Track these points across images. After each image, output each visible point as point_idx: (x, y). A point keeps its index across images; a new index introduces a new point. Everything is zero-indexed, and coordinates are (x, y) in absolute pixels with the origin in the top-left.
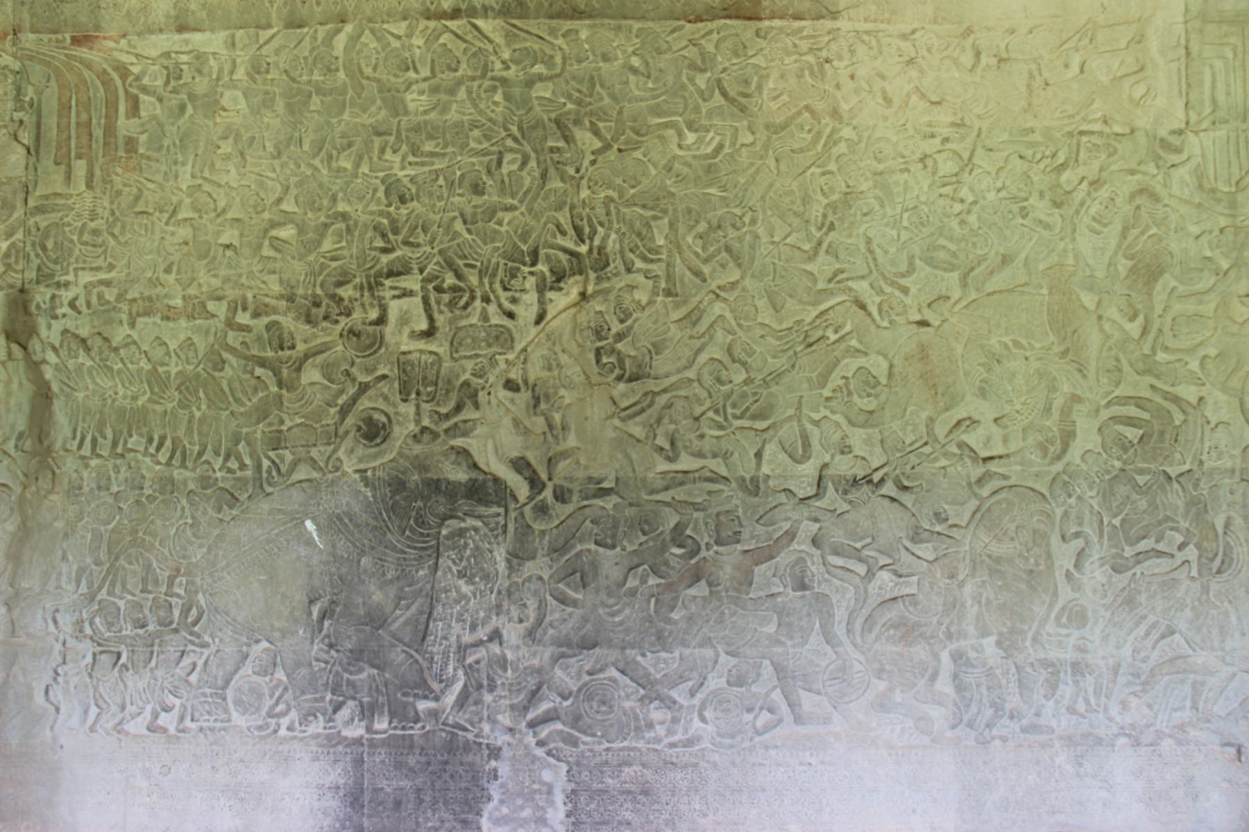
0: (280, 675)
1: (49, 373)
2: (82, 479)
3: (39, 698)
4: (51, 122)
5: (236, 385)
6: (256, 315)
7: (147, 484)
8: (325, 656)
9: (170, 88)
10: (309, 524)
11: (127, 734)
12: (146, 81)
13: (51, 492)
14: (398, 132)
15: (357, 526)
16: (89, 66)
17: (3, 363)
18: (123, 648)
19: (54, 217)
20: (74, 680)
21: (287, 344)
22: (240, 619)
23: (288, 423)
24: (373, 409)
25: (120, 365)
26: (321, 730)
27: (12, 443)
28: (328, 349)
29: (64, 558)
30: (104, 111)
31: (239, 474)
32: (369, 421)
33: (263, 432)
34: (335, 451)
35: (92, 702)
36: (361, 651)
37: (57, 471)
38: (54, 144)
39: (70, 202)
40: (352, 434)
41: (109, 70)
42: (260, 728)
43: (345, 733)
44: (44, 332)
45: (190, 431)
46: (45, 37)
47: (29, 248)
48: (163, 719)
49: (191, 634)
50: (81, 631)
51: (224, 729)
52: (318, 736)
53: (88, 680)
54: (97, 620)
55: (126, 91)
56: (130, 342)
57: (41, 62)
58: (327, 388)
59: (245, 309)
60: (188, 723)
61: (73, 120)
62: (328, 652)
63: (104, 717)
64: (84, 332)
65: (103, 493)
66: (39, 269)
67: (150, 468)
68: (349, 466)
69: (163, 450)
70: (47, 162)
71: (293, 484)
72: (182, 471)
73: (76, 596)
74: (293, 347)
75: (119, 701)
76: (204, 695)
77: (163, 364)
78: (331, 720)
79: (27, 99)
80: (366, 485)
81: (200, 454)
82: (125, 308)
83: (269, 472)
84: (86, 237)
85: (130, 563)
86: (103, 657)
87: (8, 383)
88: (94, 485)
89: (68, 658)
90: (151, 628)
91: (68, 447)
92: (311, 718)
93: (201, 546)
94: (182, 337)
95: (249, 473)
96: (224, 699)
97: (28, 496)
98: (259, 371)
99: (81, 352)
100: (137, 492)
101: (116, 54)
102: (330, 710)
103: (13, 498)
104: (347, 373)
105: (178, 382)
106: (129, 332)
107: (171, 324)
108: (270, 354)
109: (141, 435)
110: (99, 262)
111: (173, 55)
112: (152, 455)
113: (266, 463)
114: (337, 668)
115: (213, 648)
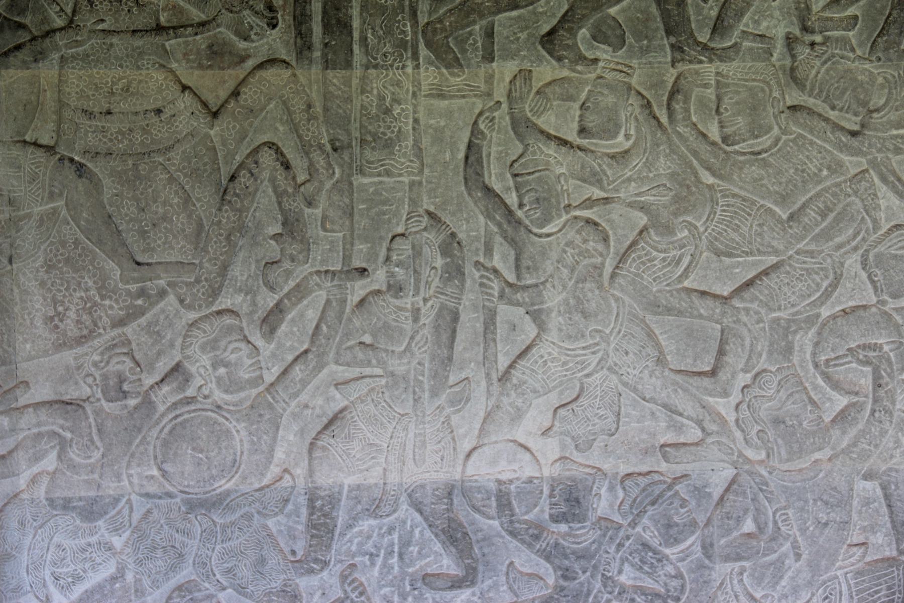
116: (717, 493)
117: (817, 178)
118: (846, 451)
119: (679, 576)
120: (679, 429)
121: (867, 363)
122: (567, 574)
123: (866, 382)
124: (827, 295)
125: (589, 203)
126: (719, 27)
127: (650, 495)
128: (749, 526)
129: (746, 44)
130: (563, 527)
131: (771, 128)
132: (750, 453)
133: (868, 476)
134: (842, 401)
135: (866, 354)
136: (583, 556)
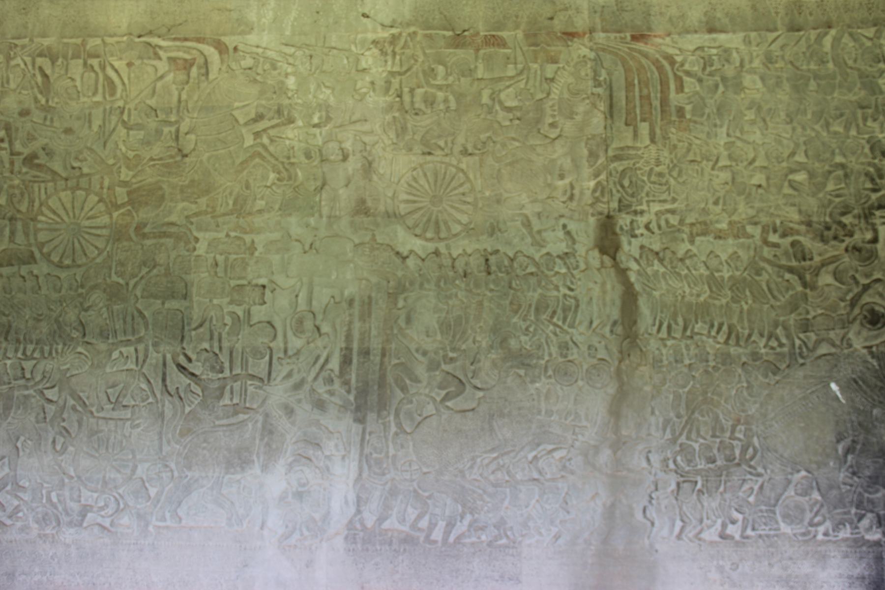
0: (816, 495)
1: (633, 278)
2: (662, 354)
3: (639, 516)
4: (621, 96)
5: (773, 286)
6: (784, 235)
7: (711, 358)
8: (850, 481)
9: (707, 72)
10: (833, 386)
11: (705, 541)
12: (687, 67)
13: (639, 365)
14: (876, 106)
15: (869, 386)
16: (646, 56)
17: (598, 270)
18: (699, 479)
19: (626, 164)
20: (664, 503)
21: (808, 257)
22: (786, 455)
23: (812, 314)
24: (874, 303)
25: (686, 271)
26: (848, 535)
27: (607, 329)
28: (839, 260)
29: (653, 413)
30: (659, 88)
31: (778, 350)
32: (872, 312)
33: (796, 320)
34: (847, 333)
35: (678, 518)
36: (877, 477)
37: (644, 349)
38: (624, 111)
39: (640, 153)
40: (858, 322)
41: (661, 59)
42: (804, 534)
43: (867, 537)
44: (625, 247)
45: (741, 319)
46: (612, 36)
47: (611, 186)
48: (731, 530)
49: (750, 467)
50: (667, 466)
51: (777, 536)
52: (845, 540)
53: (674, 501)
54: (679, 458)
55: (675, 74)
56: (689, 255)
57: (611, 52)
58: (840, 288)
59: (775, 231)
60: (749, 532)
61: (637, 94)
62: (851, 478)
63: (688, 529)
64: (656, 247)
65: (679, 365)
66: (620, 201)
67: (712, 346)
68: (858, 344)
69: (721, 333)
70: (620, 123)
71: (820, 357)
72: (736, 348)
73: (663, 441)
74: (811, 259)
75: (698, 517)
76: (761, 511)
77: (718, 271)
78: (857, 528)
79: (602, 79)
80: (873, 357)
81: (750, 336)
82: (687, 229)
83: (800, 348)
84: (653, 178)
85: (703, 416)
86: (686, 485)
87: (603, 284)
88: (672, 359)
89: (659, 486)
90: (719, 463)
91: (650, 331)
92: (841, 526)
93: (755, 402)
94: (730, 251)
95: (786, 350)
96: (775, 513)
97: (624, 367)
98: (787, 276)
99: (656, 262)
100: (705, 364)
101: (663, 48)
102: (856, 520)
103: (612, 369)
104: (853, 277)
105: (730, 284)
106: (689, 247)
107: (721, 242)
108: (794, 263)
109: (705, 322)
110: (664, 196)
111: (706, 49)
112: (715, 337)
113: (798, 342)
114: (860, 489)
115: (766, 477)
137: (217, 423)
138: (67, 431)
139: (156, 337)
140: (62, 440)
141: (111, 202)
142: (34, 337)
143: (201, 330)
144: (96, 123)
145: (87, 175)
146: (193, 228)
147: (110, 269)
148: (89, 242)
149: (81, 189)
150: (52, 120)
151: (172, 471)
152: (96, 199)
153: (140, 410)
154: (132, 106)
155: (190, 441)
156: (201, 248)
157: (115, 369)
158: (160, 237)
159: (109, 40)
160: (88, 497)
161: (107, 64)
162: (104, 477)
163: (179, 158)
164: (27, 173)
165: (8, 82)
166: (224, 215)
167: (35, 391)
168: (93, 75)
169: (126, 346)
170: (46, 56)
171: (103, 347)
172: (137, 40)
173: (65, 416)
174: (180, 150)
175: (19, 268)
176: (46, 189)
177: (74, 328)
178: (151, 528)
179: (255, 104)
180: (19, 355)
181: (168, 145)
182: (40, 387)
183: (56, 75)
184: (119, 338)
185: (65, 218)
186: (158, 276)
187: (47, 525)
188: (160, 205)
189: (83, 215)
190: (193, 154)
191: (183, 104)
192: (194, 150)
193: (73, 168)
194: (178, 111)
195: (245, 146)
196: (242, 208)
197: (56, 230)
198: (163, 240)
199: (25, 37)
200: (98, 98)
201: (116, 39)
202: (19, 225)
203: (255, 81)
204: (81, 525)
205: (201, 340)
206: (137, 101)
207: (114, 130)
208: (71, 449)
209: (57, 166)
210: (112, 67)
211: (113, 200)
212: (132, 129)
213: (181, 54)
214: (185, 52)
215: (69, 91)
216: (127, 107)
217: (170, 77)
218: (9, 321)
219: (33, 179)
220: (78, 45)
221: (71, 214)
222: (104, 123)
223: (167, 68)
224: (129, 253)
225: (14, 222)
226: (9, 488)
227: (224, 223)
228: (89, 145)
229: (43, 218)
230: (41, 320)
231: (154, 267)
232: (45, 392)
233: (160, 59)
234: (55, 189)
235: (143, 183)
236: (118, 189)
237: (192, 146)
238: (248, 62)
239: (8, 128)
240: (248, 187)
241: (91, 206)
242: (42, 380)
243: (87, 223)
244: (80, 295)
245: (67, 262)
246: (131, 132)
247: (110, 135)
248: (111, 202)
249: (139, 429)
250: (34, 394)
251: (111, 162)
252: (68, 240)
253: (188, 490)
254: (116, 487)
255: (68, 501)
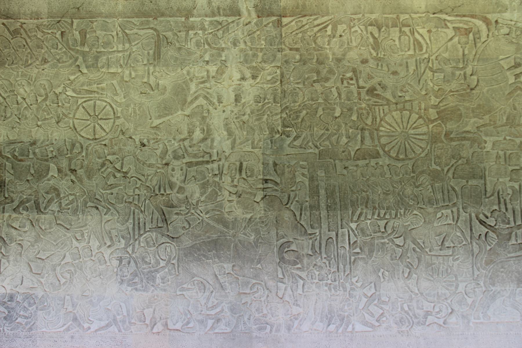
116: (40, 297)
117: (61, 237)
118: (64, 290)
119: (31, 313)
120: (34, 284)
121: (69, 273)
122: (9, 312)
123: (69, 277)
124: (62, 260)
125: (20, 240)
126: (45, 208)
127: (27, 297)
128: (46, 304)
129: (50, 212)
130: (10, 303)
131: (53, 228)
132: (46, 290)
133: (68, 295)
134: (64, 280)
135: (69, 271)
136: (12, 309)
137: (509, 255)
138: (412, 265)
139: (466, 203)
140: (408, 270)
141: (427, 118)
142: (385, 205)
143: (492, 198)
144: (412, 68)
145: (409, 101)
146: (482, 134)
147: (431, 161)
148: (415, 144)
149: (406, 110)
150: (382, 65)
151: (481, 287)
152: (417, 116)
153: (458, 249)
154: (433, 57)
155: (493, 267)
156: (489, 146)
157: (439, 224)
158: (462, 140)
159: (414, 16)
160: (427, 306)
161: (415, 31)
162: (438, 293)
163: (469, 91)
164: (370, 100)
165: (351, 42)
166: (502, 126)
167: (388, 240)
168: (407, 37)
169: (446, 209)
170: (375, 26)
171: (430, 210)
172: (432, 16)
173: (409, 255)
174: (469, 86)
175: (370, 161)
176: (383, 110)
177: (411, 199)
178: (471, 324)
179: (513, 57)
180: (376, 217)
181: (460, 82)
182: (392, 237)
183: (382, 38)
184: (441, 205)
185: (398, 129)
186: (463, 164)
187: (403, 325)
188: (460, 120)
189: (409, 126)
190: (477, 88)
191: (466, 57)
192: (477, 85)
193: (400, 97)
194: (464, 61)
195: (510, 83)
196: (513, 122)
197: (393, 136)
198: (463, 142)
199: (360, 13)
200: (411, 52)
201: (418, 15)
202: (367, 133)
203: (512, 42)
204: (425, 324)
205: (493, 204)
206: (436, 55)
207: (424, 72)
208: (414, 275)
209: (388, 95)
210: (419, 33)
211: (429, 117)
212: (436, 72)
213: (461, 25)
214: (464, 24)
215: (392, 48)
216: (431, 58)
217: (456, 39)
218: (367, 195)
219: (374, 104)
220: (394, 19)
221: (401, 126)
222: (417, 68)
223: (453, 34)
224: (443, 151)
225: (364, 131)
226: (376, 302)
227: (502, 131)
228: (409, 82)
229: (383, 129)
230: (389, 194)
231: (460, 159)
232: (395, 240)
233: (449, 28)
234: (389, 110)
235: (448, 106)
236: (430, 110)
237: (476, 83)
238: (506, 30)
239: (354, 71)
240: (515, 109)
241: (414, 121)
242: (393, 232)
243: (412, 132)
244: (413, 177)
245: (401, 157)
246: (435, 74)
247: (422, 76)
248: (427, 118)
249: (458, 262)
250: (388, 242)
251: (424, 93)
252: (401, 143)
253: (493, 298)
254: (446, 299)
255: (415, 309)
